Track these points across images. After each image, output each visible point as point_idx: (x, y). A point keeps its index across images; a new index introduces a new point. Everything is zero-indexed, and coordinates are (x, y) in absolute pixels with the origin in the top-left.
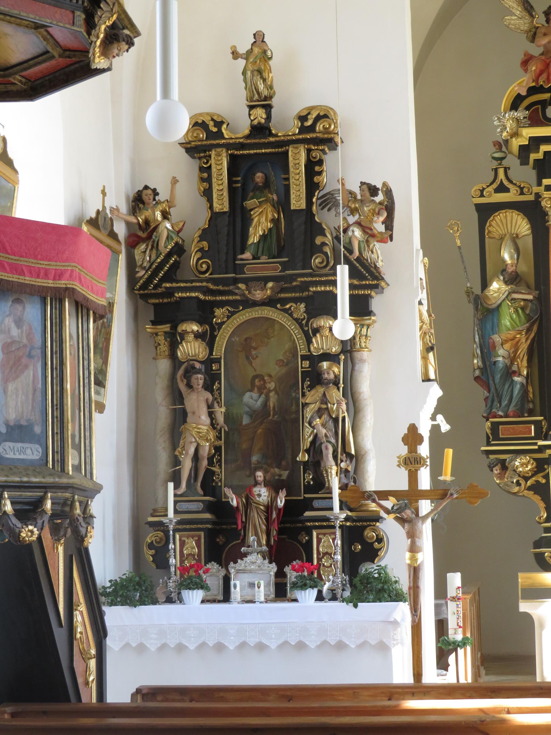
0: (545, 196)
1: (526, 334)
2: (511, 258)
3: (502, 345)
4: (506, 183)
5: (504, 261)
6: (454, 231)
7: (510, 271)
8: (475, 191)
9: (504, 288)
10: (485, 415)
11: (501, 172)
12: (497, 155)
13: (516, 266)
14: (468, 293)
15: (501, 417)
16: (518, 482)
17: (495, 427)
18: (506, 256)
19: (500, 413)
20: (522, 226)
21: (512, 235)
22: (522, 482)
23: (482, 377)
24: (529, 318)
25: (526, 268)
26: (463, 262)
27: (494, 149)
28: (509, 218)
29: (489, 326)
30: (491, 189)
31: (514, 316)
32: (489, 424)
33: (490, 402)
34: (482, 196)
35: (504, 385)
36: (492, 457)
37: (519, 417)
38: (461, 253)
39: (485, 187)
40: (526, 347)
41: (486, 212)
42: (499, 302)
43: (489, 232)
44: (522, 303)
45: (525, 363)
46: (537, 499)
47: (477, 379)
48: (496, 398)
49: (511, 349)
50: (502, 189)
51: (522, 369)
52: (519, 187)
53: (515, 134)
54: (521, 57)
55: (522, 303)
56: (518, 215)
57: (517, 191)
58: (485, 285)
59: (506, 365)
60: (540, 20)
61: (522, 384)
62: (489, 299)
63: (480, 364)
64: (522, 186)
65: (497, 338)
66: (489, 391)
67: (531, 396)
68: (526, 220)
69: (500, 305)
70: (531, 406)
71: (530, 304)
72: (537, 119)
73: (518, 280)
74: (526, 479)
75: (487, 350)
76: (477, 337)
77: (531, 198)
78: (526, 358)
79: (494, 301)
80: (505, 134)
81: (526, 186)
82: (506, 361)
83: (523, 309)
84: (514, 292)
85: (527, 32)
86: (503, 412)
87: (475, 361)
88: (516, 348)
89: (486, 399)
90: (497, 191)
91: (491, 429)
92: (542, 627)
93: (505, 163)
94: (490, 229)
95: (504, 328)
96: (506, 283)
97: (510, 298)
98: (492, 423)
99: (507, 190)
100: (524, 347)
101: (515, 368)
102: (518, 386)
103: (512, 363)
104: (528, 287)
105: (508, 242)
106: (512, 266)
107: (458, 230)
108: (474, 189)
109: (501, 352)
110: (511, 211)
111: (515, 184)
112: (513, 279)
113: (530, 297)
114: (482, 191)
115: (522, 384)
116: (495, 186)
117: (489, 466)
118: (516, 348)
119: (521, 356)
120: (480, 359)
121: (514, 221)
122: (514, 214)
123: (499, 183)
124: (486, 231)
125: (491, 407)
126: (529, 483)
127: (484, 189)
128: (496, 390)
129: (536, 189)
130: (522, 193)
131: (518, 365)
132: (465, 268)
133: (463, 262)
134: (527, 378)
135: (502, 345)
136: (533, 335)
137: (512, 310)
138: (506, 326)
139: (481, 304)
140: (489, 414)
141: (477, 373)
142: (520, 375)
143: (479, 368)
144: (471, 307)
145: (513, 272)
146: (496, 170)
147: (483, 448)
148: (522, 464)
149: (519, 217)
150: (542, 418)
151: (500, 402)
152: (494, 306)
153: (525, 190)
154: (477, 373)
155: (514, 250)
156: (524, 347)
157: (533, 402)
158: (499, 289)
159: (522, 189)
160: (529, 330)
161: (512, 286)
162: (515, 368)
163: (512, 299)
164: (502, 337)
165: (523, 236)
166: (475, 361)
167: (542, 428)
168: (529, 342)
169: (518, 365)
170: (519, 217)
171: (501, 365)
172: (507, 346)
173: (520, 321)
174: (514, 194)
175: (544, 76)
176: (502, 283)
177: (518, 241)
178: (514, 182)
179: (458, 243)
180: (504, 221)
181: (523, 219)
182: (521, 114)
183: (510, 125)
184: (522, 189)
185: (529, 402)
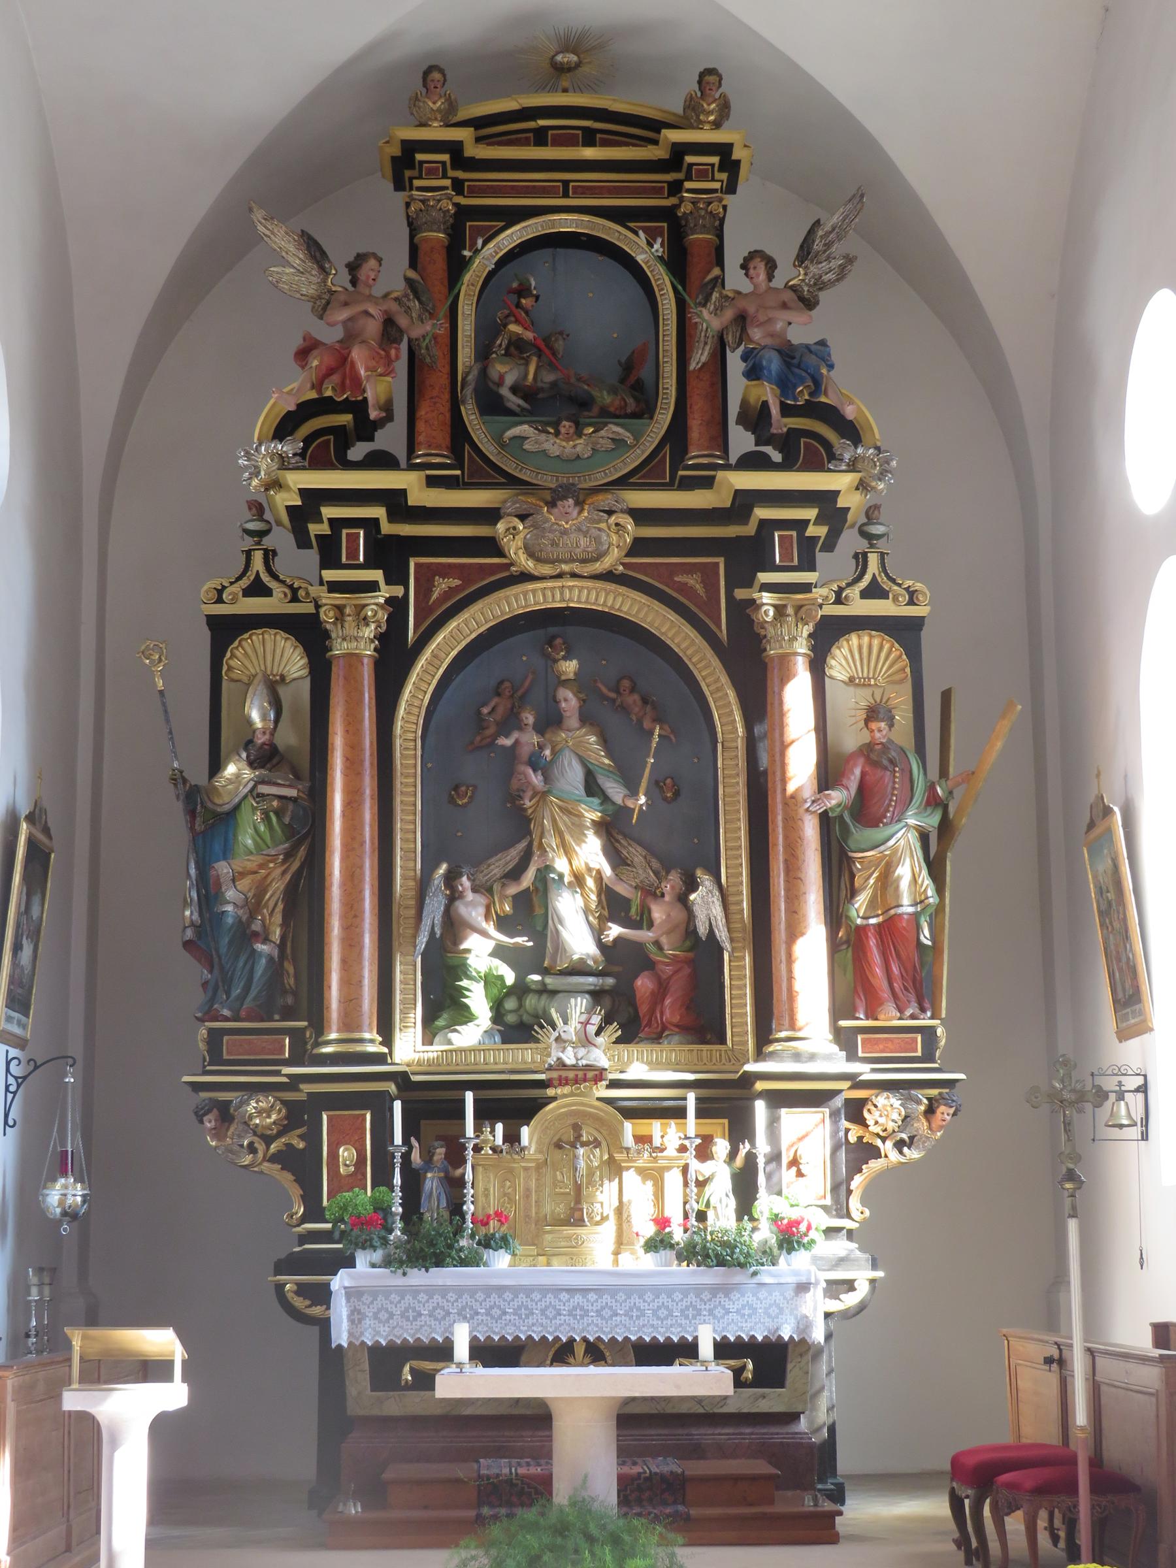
0: (324, 601)
1: (284, 861)
2: (264, 718)
3: (234, 881)
4: (265, 578)
5: (249, 722)
6: (152, 661)
7: (260, 741)
8: (207, 592)
9: (248, 774)
10: (199, 1015)
11: (258, 557)
12: (251, 526)
13: (272, 734)
14: (178, 779)
15: (227, 1019)
16: (251, 1144)
17: (215, 1038)
18: (255, 716)
19: (226, 1012)
20: (292, 660)
21: (266, 676)
22: (260, 1147)
23: (199, 943)
24: (289, 831)
25: (291, 737)
26: (168, 721)
27: (249, 516)
28: (269, 646)
29: (217, 847)
30: (237, 588)
31: (262, 828)
32: (203, 1032)
33: (212, 990)
34: (220, 600)
35: (237, 957)
36: (204, 1095)
37: (262, 1021)
38: (164, 704)
39: (226, 584)
40: (282, 888)
41: (226, 631)
42: (237, 800)
43: (230, 668)
44: (275, 803)
45: (278, 918)
46: (286, 1179)
47: (187, 944)
48: (220, 984)
49: (249, 891)
50: (257, 589)
51: (272, 928)
52: (291, 587)
53: (275, 484)
54: (297, 342)
55: (275, 803)
56: (287, 639)
57: (285, 595)
58: (216, 767)
59: (240, 921)
60: (339, 279)
61: (270, 959)
62: (219, 795)
63: (196, 917)
64: (296, 586)
65: (223, 869)
66: (211, 972)
67: (292, 981)
68: (300, 649)
69: (237, 807)
70: (290, 1000)
71: (291, 806)
72: (314, 459)
73: (275, 761)
74: (268, 1140)
75: (209, 895)
76: (192, 865)
77: (308, 608)
78: (280, 906)
79: (226, 800)
80: (255, 482)
81: (303, 585)
82: (240, 912)
83: (278, 813)
84: (263, 782)
85: (314, 299)
86: (230, 1009)
87: (187, 913)
88: (261, 890)
89: (205, 985)
90: (249, 592)
91: (208, 1043)
92: (114, 1444)
93: (268, 542)
94: (231, 663)
95: (241, 849)
96: (251, 764)
97: (255, 794)
98: (211, 1031)
99: (268, 592)
100: (278, 888)
101: (256, 926)
102: (264, 961)
103: (252, 917)
104: (298, 777)
105: (260, 688)
106: (264, 733)
107: (160, 660)
108: (205, 588)
109: (230, 894)
110: (273, 631)
111: (283, 582)
112: (266, 757)
113: (292, 793)
114: (220, 592)
115: (270, 959)
116: (245, 583)
117: (196, 1113)
118: (261, 890)
119: (271, 904)
120: (195, 907)
121: (278, 652)
122: (278, 637)
123: (252, 578)
124: (225, 668)
125: (212, 1000)
126: (273, 1148)
127: (224, 588)
128: (222, 968)
129: (318, 591)
130: (295, 599)
131: (263, 921)
132: (171, 733)
133: (168, 721)
134: (282, 946)
135: (234, 881)
136: (296, 865)
137: (258, 817)
138: (246, 846)
139: (202, 803)
140: (206, 1013)
141: (189, 934)
142: (266, 940)
143: (192, 924)
144: (179, 807)
145: (264, 744)
146: (248, 554)
147: (186, 1079)
148: (260, 1111)
149: (289, 644)
150: (306, 1023)
151: (228, 994)
152: (227, 808)
153: (301, 593)
154: (189, 934)
155: (270, 703)
156: (277, 887)
157: (295, 994)
158: (238, 776)
159: (294, 591)
160: (289, 855)
161: (263, 772)
162: (256, 926)
163: (259, 795)
164: (234, 867)
165: (294, 679)
166: (187, 913)
167: (306, 1043)
168: (288, 877)
169: (263, 921)
170: (289, 644)
171: (230, 920)
172: (245, 884)
173: (272, 837)
174: (280, 600)
175: (336, 378)
176: (243, 764)
177: (283, 691)
178: (281, 577)
179: (160, 684)
180: (260, 651)
181: (296, 647)
182: (287, 448)
183: (266, 465)
184: (294, 591)
185: (284, 992)
